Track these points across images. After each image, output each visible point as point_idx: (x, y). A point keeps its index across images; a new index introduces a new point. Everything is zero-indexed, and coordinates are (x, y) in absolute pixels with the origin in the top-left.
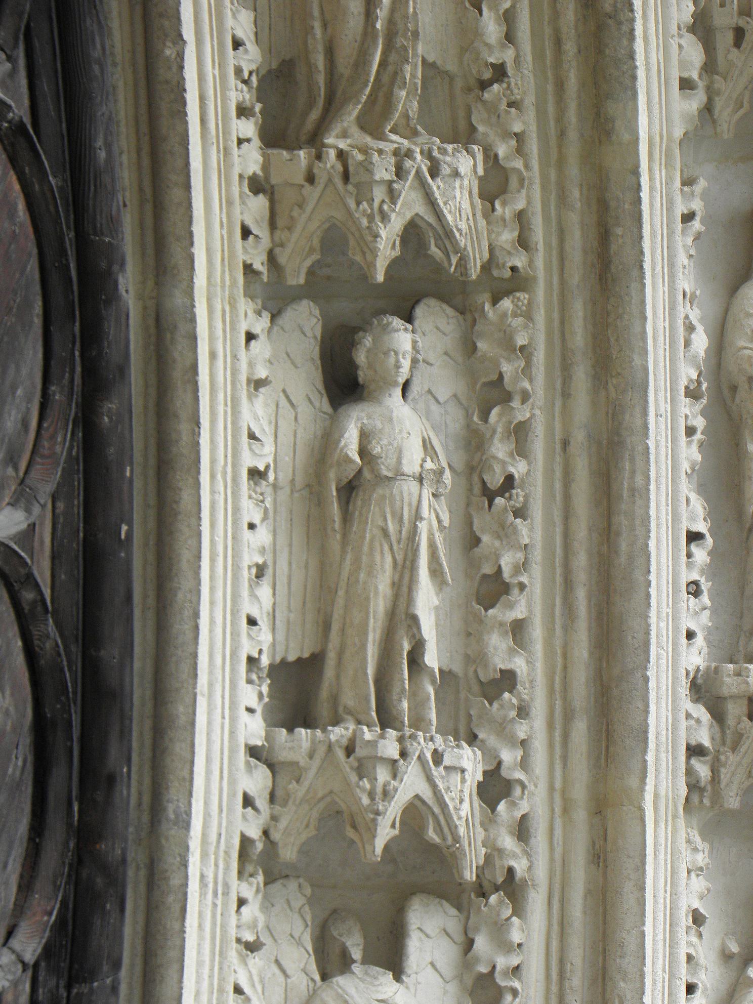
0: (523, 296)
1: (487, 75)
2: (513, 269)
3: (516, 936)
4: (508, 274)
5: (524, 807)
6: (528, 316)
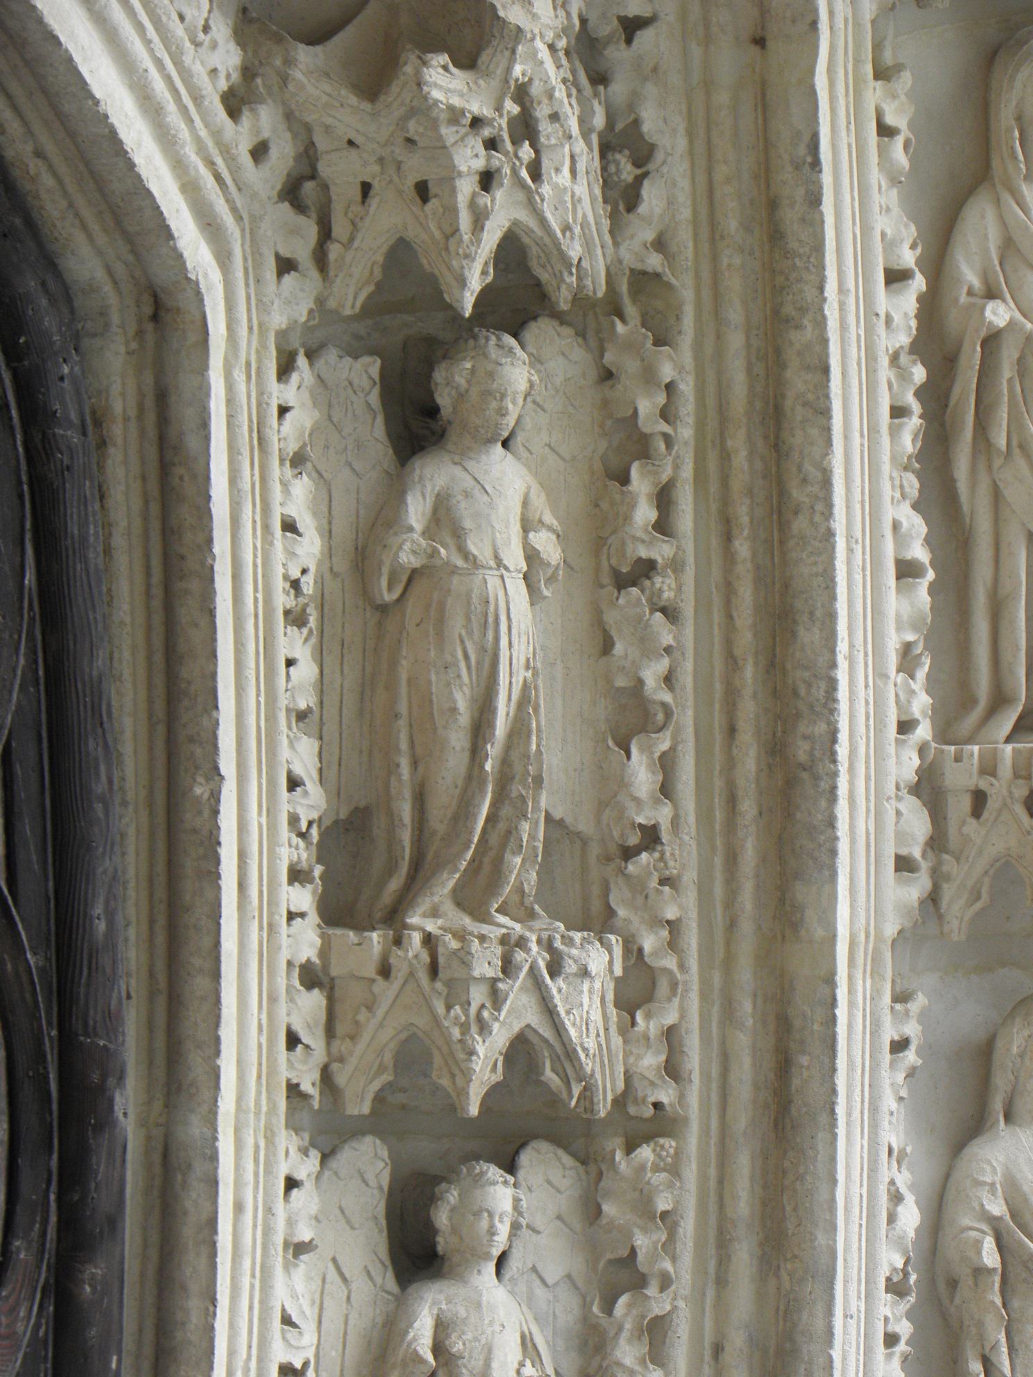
0: (669, 1144)
1: (634, 839)
2: (657, 1106)
4: (649, 1112)
6: (674, 1170)
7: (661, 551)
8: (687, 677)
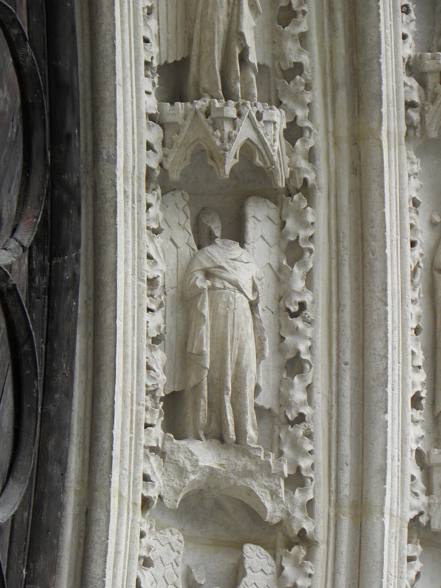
3: (310, 218)
5: (311, 143)
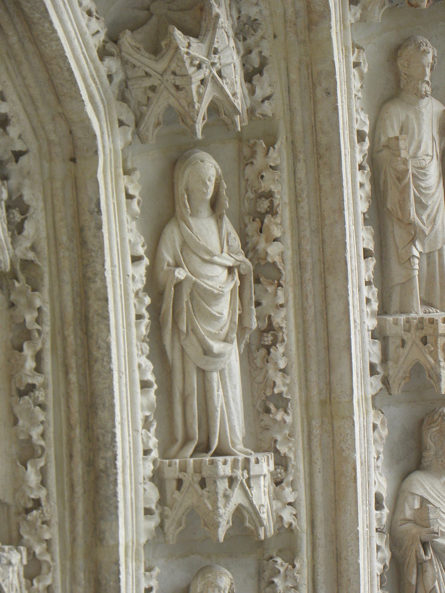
1: (30, 505)
7: (38, 380)
8: (51, 434)
